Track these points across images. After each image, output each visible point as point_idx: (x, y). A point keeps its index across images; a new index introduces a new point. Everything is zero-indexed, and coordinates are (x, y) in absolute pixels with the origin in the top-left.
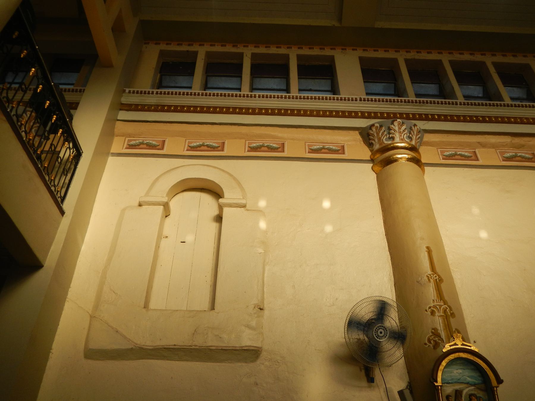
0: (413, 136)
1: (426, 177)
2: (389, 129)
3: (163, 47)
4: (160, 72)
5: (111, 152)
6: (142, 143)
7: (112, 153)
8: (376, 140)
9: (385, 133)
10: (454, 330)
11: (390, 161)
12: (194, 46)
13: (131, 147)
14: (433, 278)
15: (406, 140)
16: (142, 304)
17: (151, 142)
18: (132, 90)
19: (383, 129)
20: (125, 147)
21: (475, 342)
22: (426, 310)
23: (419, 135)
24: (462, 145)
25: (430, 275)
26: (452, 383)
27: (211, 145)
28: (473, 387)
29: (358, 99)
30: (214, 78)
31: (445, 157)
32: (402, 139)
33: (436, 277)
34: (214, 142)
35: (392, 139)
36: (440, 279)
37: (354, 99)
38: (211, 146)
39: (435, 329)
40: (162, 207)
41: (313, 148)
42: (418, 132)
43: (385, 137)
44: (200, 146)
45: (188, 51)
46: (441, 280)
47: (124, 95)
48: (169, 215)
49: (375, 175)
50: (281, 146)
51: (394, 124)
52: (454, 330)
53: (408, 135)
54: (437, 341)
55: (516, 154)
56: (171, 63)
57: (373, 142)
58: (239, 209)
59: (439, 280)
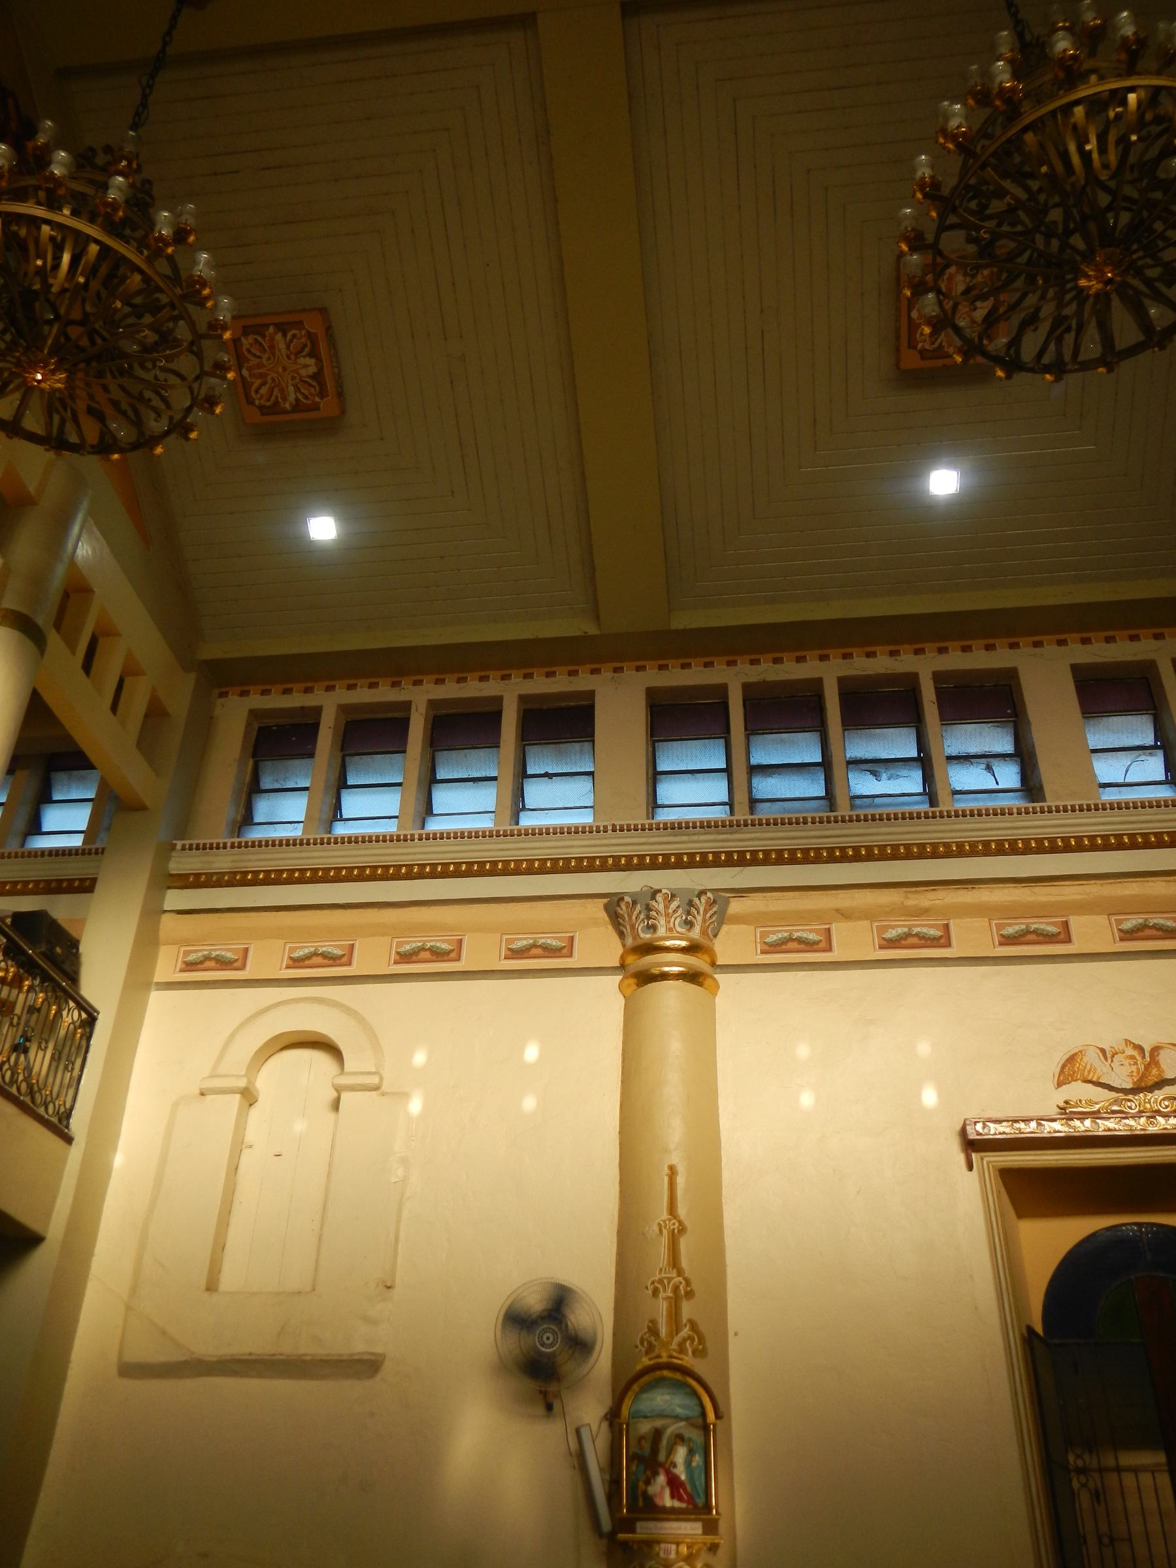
0: (695, 918)
1: (721, 1002)
2: (648, 908)
3: (257, 701)
4: (254, 755)
5: (156, 980)
6: (207, 958)
7: (157, 984)
8: (628, 927)
9: (642, 916)
10: (684, 1321)
11: (646, 978)
12: (316, 692)
13: (189, 968)
14: (668, 1227)
15: (679, 930)
16: (203, 1285)
17: (223, 953)
18: (187, 842)
19: (638, 907)
20: (178, 969)
21: (736, 1334)
22: (647, 1288)
23: (715, 909)
24: (803, 917)
25: (664, 1221)
26: (651, 1417)
27: (329, 953)
28: (682, 1424)
29: (610, 828)
30: (357, 758)
31: (767, 947)
32: (672, 928)
33: (674, 1224)
34: (335, 946)
35: (652, 930)
36: (681, 1228)
37: (602, 828)
38: (329, 956)
39: (653, 1322)
40: (238, 1096)
41: (514, 947)
42: (710, 906)
43: (642, 925)
44: (309, 957)
45: (302, 708)
46: (682, 1229)
47: (174, 854)
48: (256, 1101)
49: (623, 1001)
50: (455, 948)
51: (657, 899)
52: (684, 1321)
53: (684, 918)
54: (653, 1342)
55: (910, 929)
56: (275, 728)
57: (624, 930)
58: (368, 1093)
59: (679, 1231)
